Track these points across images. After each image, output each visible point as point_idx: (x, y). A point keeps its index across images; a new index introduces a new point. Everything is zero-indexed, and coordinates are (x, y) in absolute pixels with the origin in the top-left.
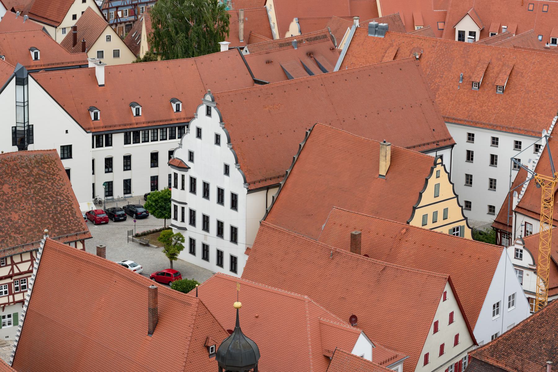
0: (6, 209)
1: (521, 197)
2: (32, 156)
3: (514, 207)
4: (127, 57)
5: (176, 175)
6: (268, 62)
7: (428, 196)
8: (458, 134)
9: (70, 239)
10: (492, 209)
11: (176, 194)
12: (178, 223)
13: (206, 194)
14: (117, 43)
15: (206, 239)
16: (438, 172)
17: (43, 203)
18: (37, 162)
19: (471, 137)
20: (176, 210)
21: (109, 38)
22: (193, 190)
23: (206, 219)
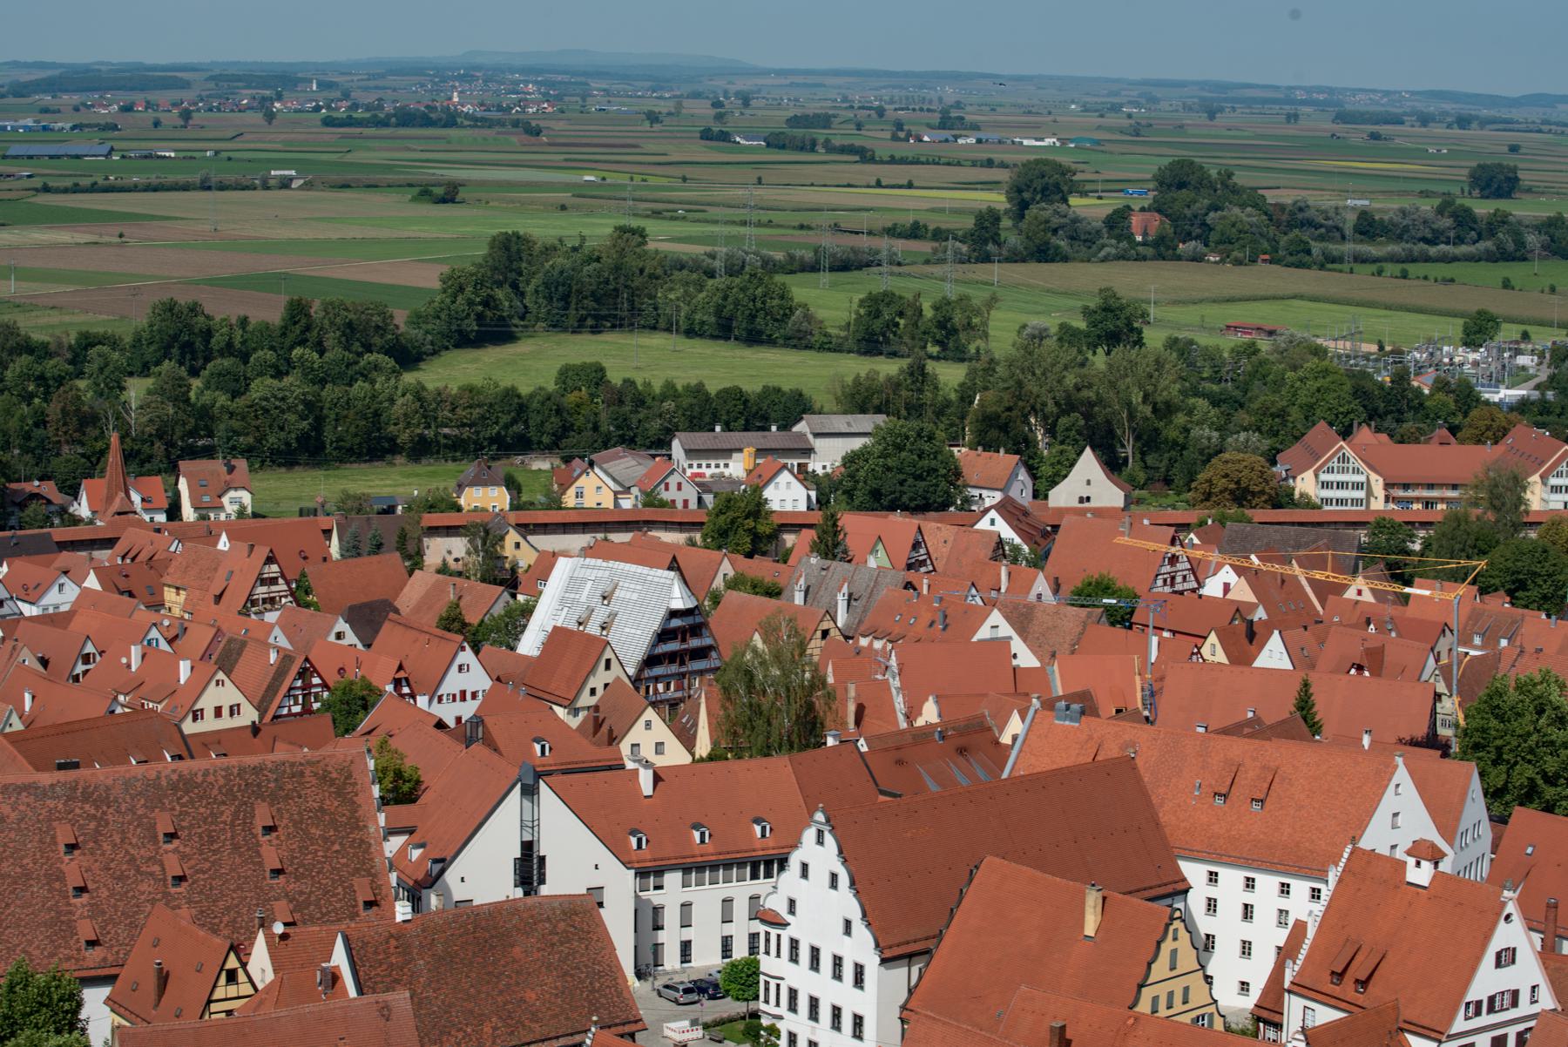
0: (518, 984)
1: (1297, 968)
2: (556, 905)
3: (1287, 985)
4: (676, 755)
5: (767, 934)
6: (900, 762)
7: (1160, 969)
8: (1194, 872)
9: (621, 1029)
10: (1244, 986)
11: (768, 964)
12: (770, 1008)
13: (815, 963)
14: (661, 731)
15: (813, 1033)
16: (1176, 930)
17: (572, 976)
18: (564, 913)
19: (1213, 878)
20: (767, 990)
21: (648, 725)
22: (794, 958)
23: (814, 1003)
